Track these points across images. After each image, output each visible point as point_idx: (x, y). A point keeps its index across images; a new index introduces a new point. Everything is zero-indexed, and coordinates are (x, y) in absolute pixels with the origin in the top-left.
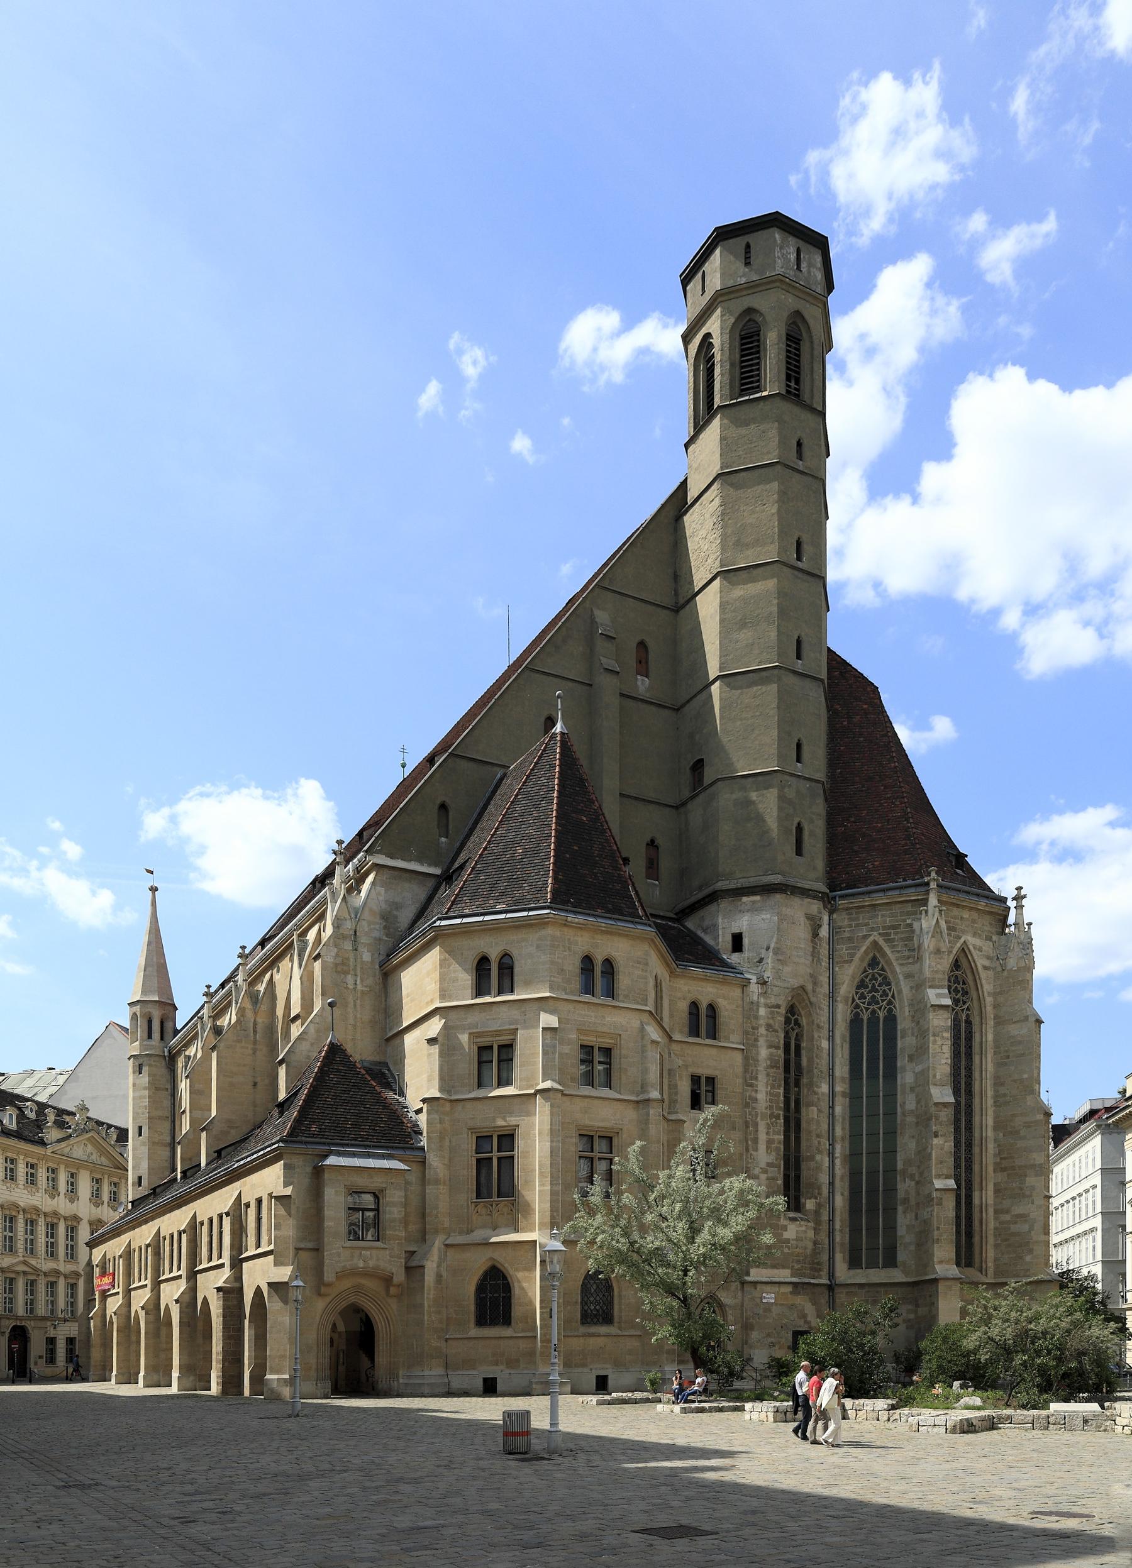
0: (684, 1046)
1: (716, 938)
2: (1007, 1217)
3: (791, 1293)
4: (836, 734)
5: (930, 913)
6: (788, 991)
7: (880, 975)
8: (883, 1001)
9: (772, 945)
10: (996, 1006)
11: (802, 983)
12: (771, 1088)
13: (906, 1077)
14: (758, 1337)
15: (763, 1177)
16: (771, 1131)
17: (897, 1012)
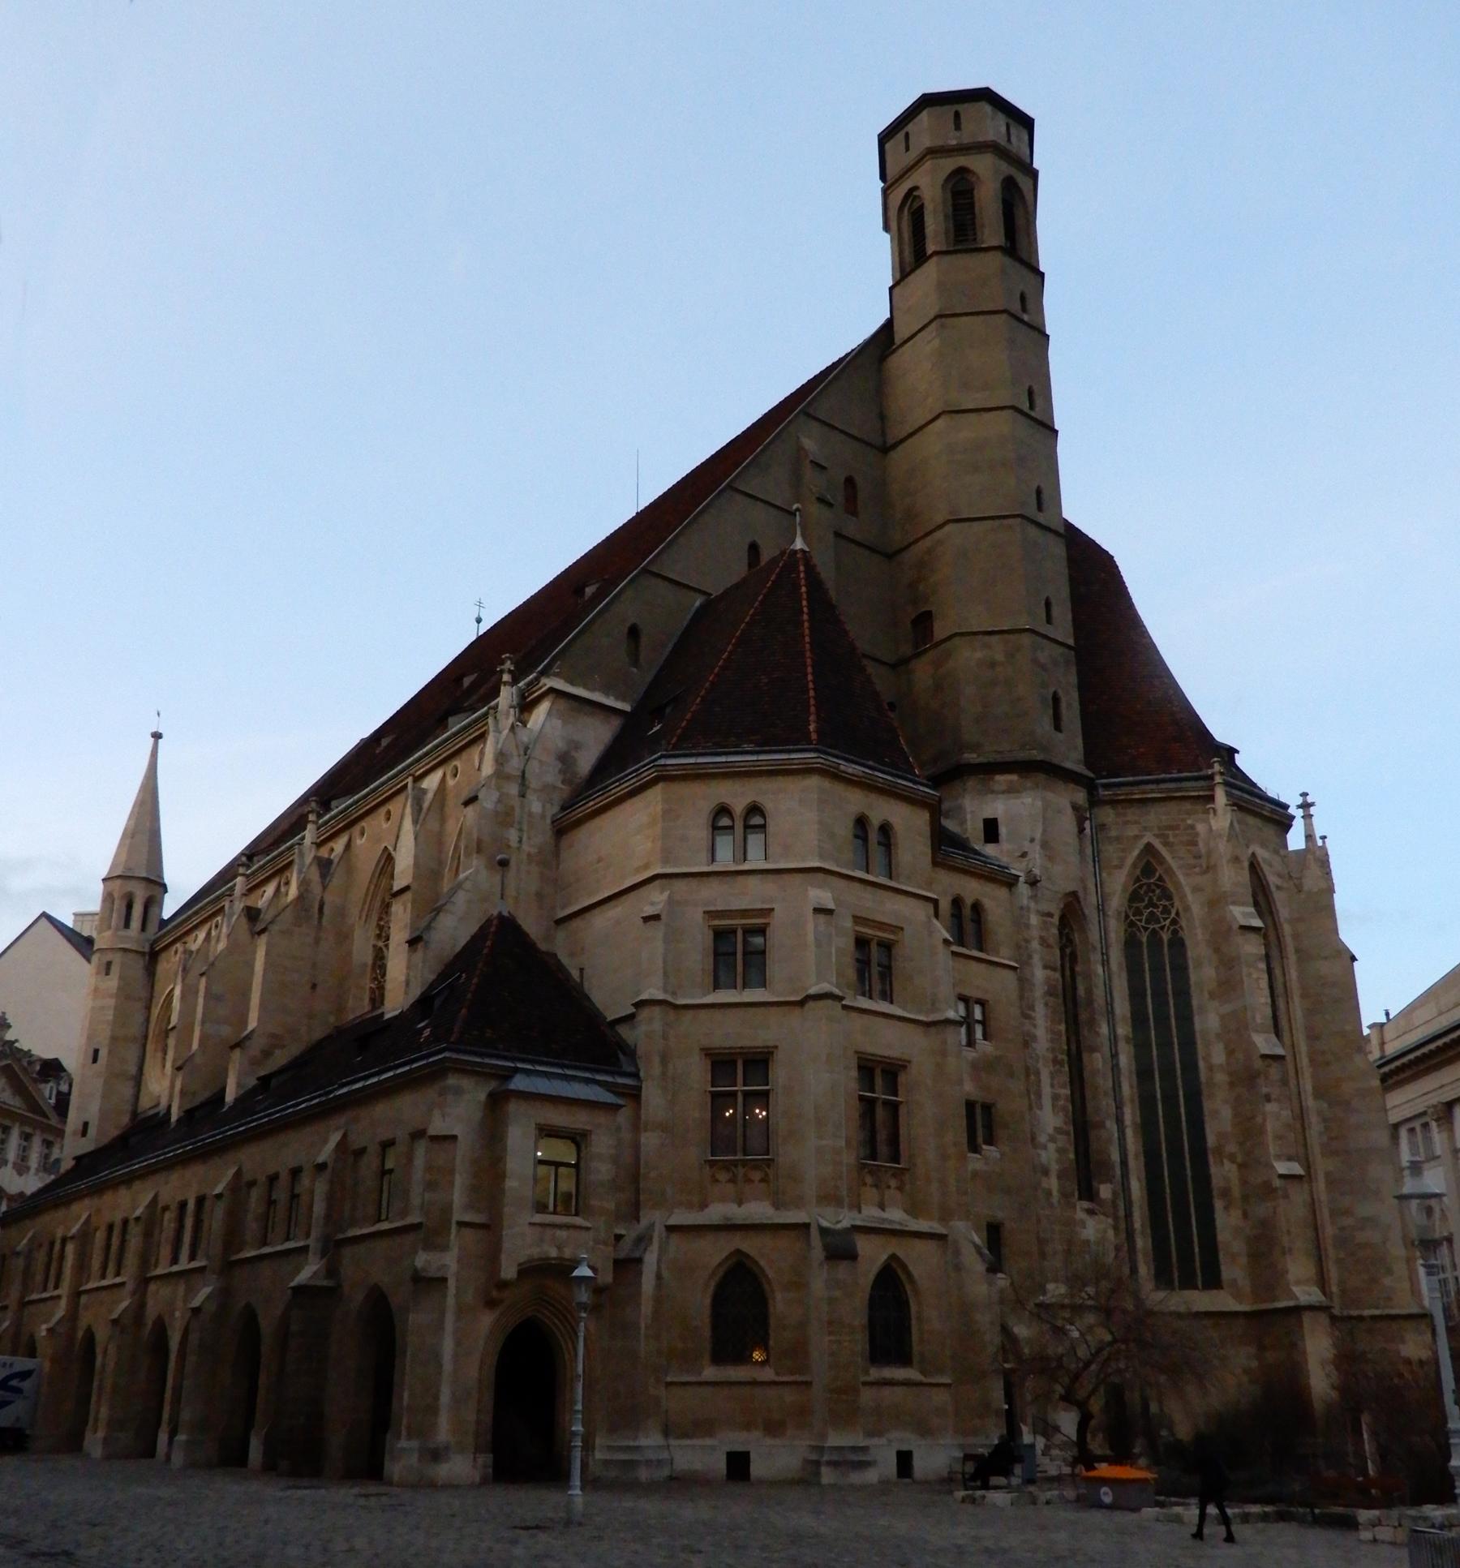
1: (963, 822)
2: (1348, 1221)
4: (1078, 601)
5: (1220, 811)
7: (1158, 886)
8: (1165, 919)
9: (1038, 836)
10: (1296, 936)
13: (1208, 1020)
15: (1052, 1147)
17: (1185, 935)
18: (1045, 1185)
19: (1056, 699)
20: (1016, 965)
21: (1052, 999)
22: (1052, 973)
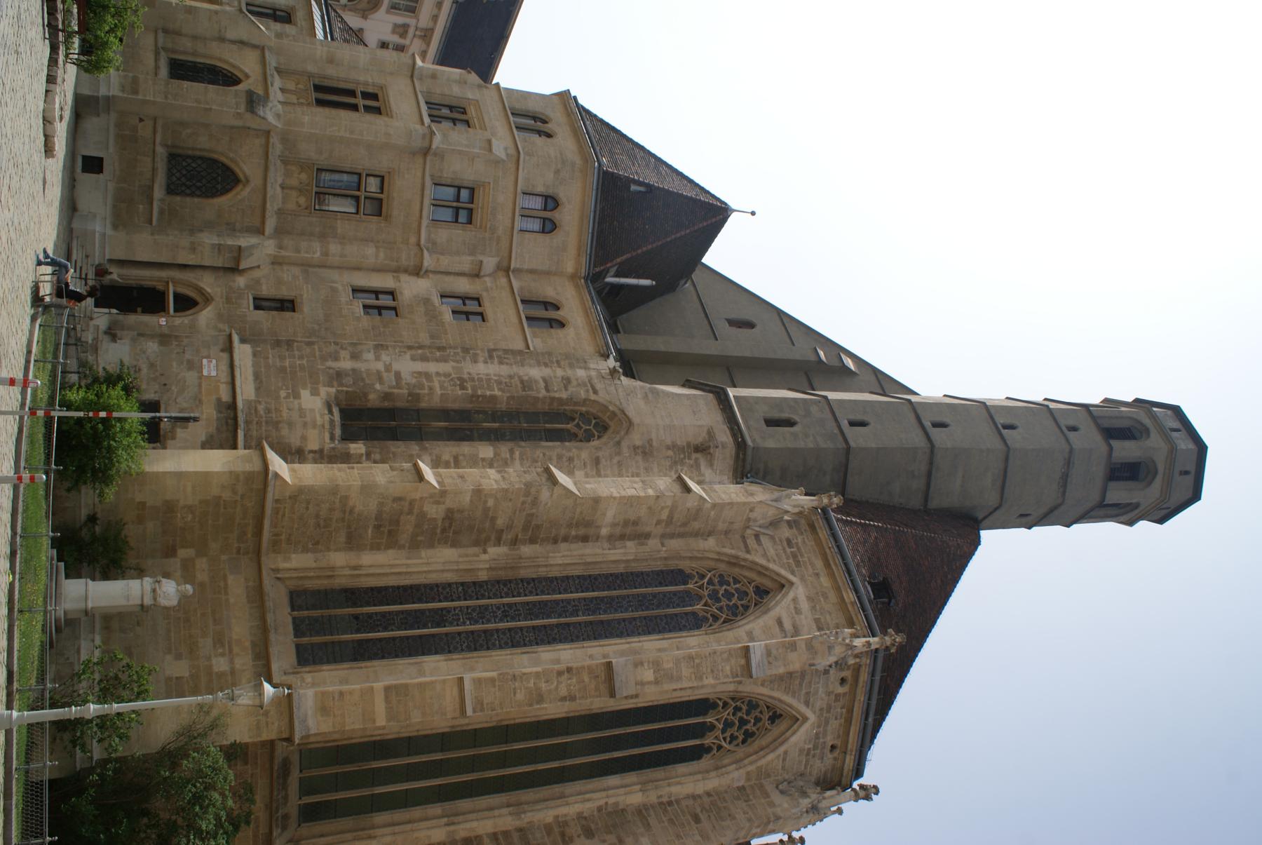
0: (508, 289)
3: (219, 400)
6: (618, 403)
11: (636, 420)
12: (495, 380)
14: (150, 350)
16: (443, 378)
18: (343, 354)
19: (790, 423)
20: (532, 348)
21: (520, 385)
22: (543, 387)
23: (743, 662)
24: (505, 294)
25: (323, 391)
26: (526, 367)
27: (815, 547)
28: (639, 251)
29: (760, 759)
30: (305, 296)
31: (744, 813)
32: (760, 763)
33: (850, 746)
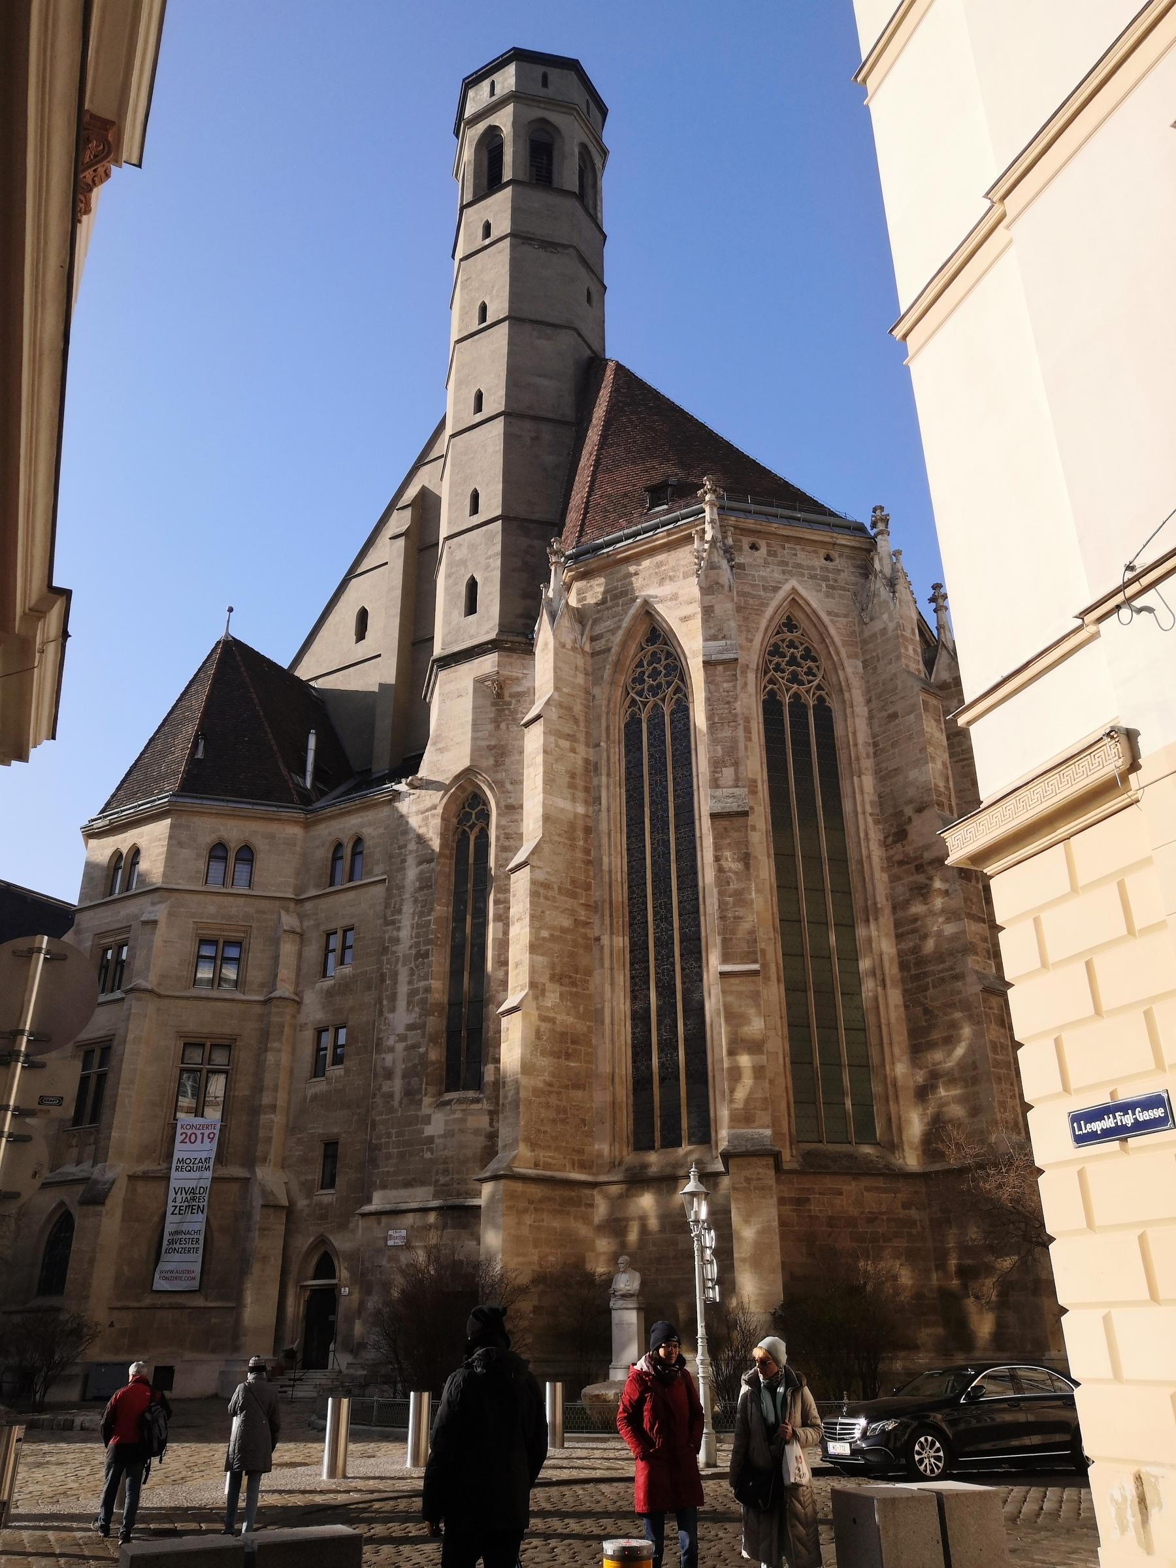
0: (317, 901)
12: (420, 918)
23: (720, 668)
24: (324, 904)
25: (425, 1110)
26: (406, 884)
27: (607, 572)
28: (275, 748)
29: (833, 643)
30: (320, 1131)
31: (890, 663)
32: (839, 643)
33: (827, 539)
